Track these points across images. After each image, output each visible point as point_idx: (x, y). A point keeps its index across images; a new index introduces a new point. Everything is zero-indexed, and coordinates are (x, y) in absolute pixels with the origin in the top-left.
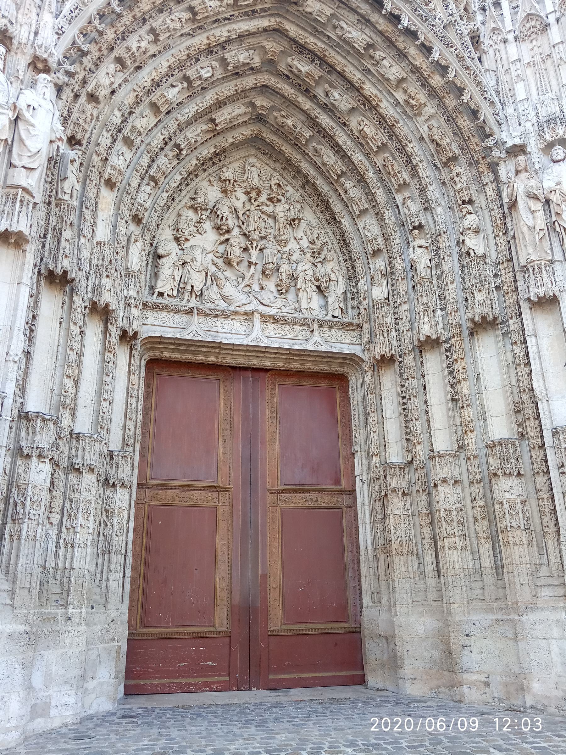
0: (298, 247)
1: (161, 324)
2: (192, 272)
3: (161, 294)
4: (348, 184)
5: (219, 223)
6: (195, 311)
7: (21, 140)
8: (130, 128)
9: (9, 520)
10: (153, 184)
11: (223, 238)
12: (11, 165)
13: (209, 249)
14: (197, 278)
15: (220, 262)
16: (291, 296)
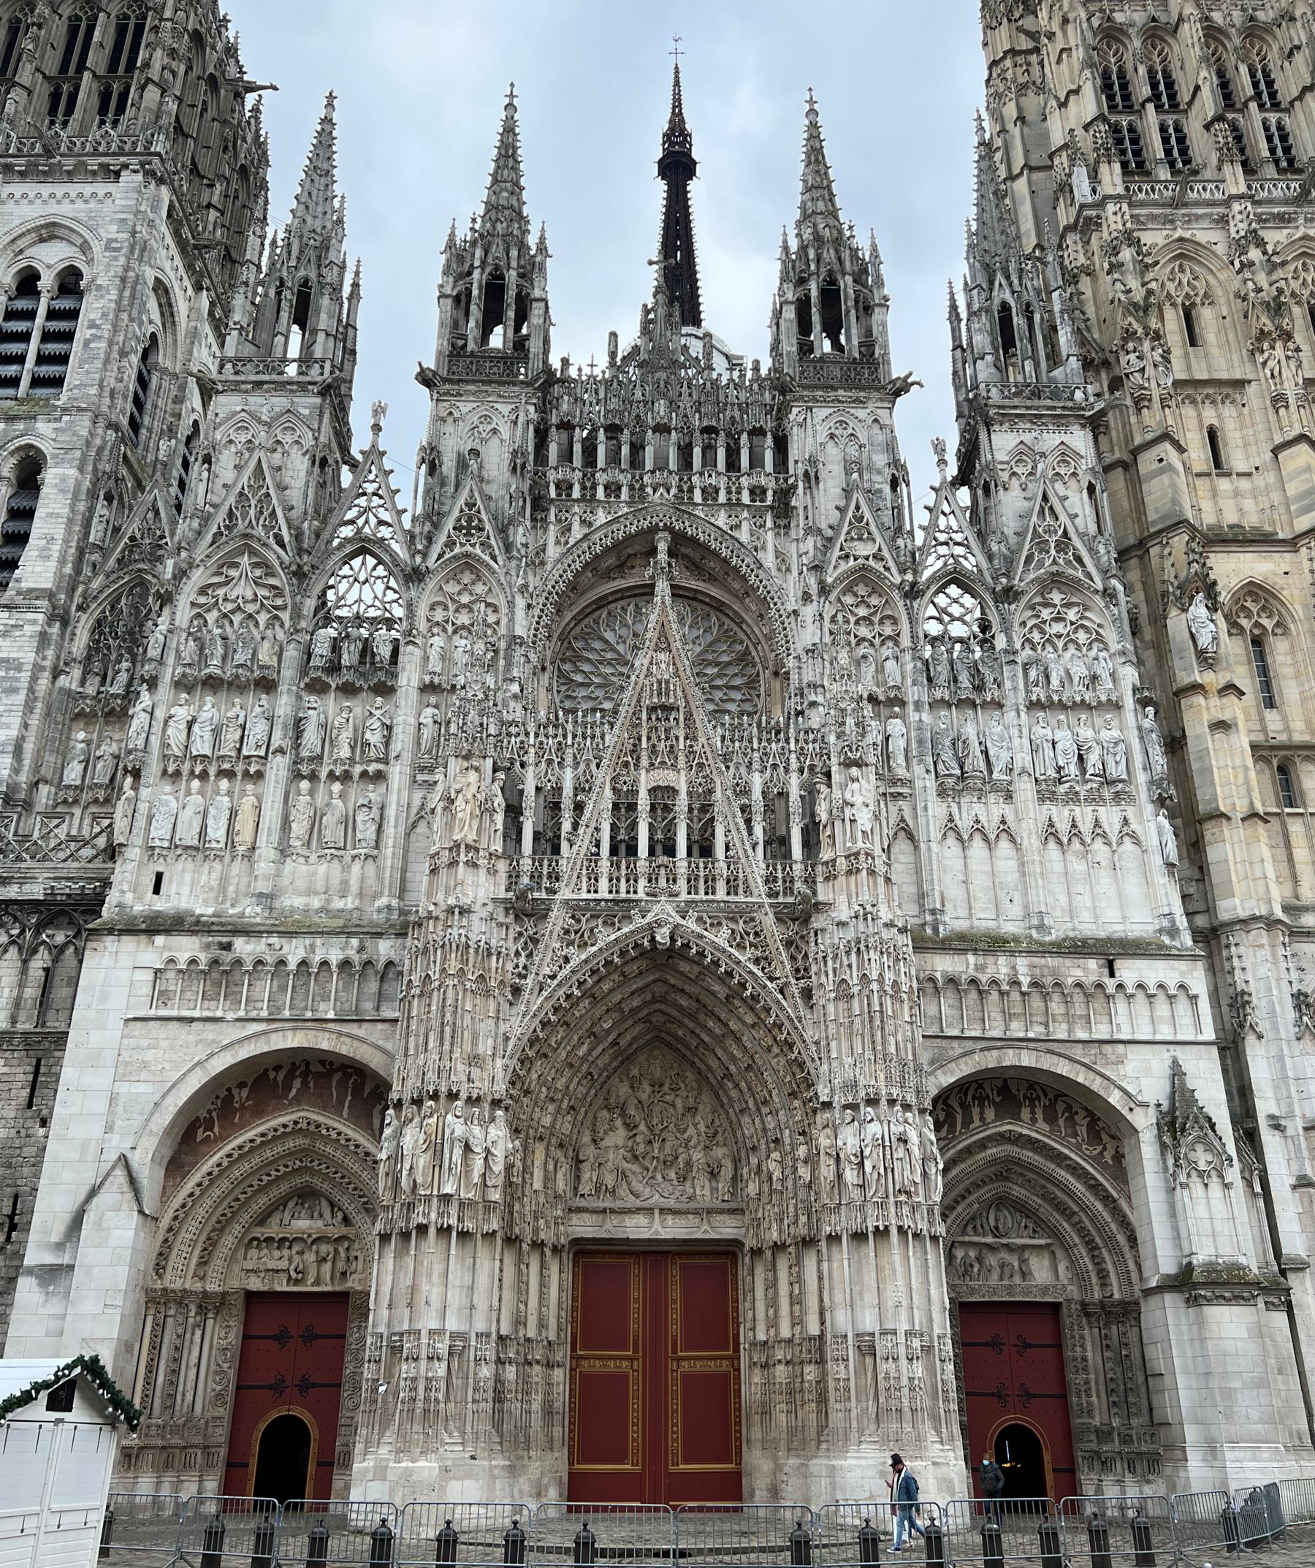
4: (730, 1085)
15: (628, 1155)
16: (688, 1184)
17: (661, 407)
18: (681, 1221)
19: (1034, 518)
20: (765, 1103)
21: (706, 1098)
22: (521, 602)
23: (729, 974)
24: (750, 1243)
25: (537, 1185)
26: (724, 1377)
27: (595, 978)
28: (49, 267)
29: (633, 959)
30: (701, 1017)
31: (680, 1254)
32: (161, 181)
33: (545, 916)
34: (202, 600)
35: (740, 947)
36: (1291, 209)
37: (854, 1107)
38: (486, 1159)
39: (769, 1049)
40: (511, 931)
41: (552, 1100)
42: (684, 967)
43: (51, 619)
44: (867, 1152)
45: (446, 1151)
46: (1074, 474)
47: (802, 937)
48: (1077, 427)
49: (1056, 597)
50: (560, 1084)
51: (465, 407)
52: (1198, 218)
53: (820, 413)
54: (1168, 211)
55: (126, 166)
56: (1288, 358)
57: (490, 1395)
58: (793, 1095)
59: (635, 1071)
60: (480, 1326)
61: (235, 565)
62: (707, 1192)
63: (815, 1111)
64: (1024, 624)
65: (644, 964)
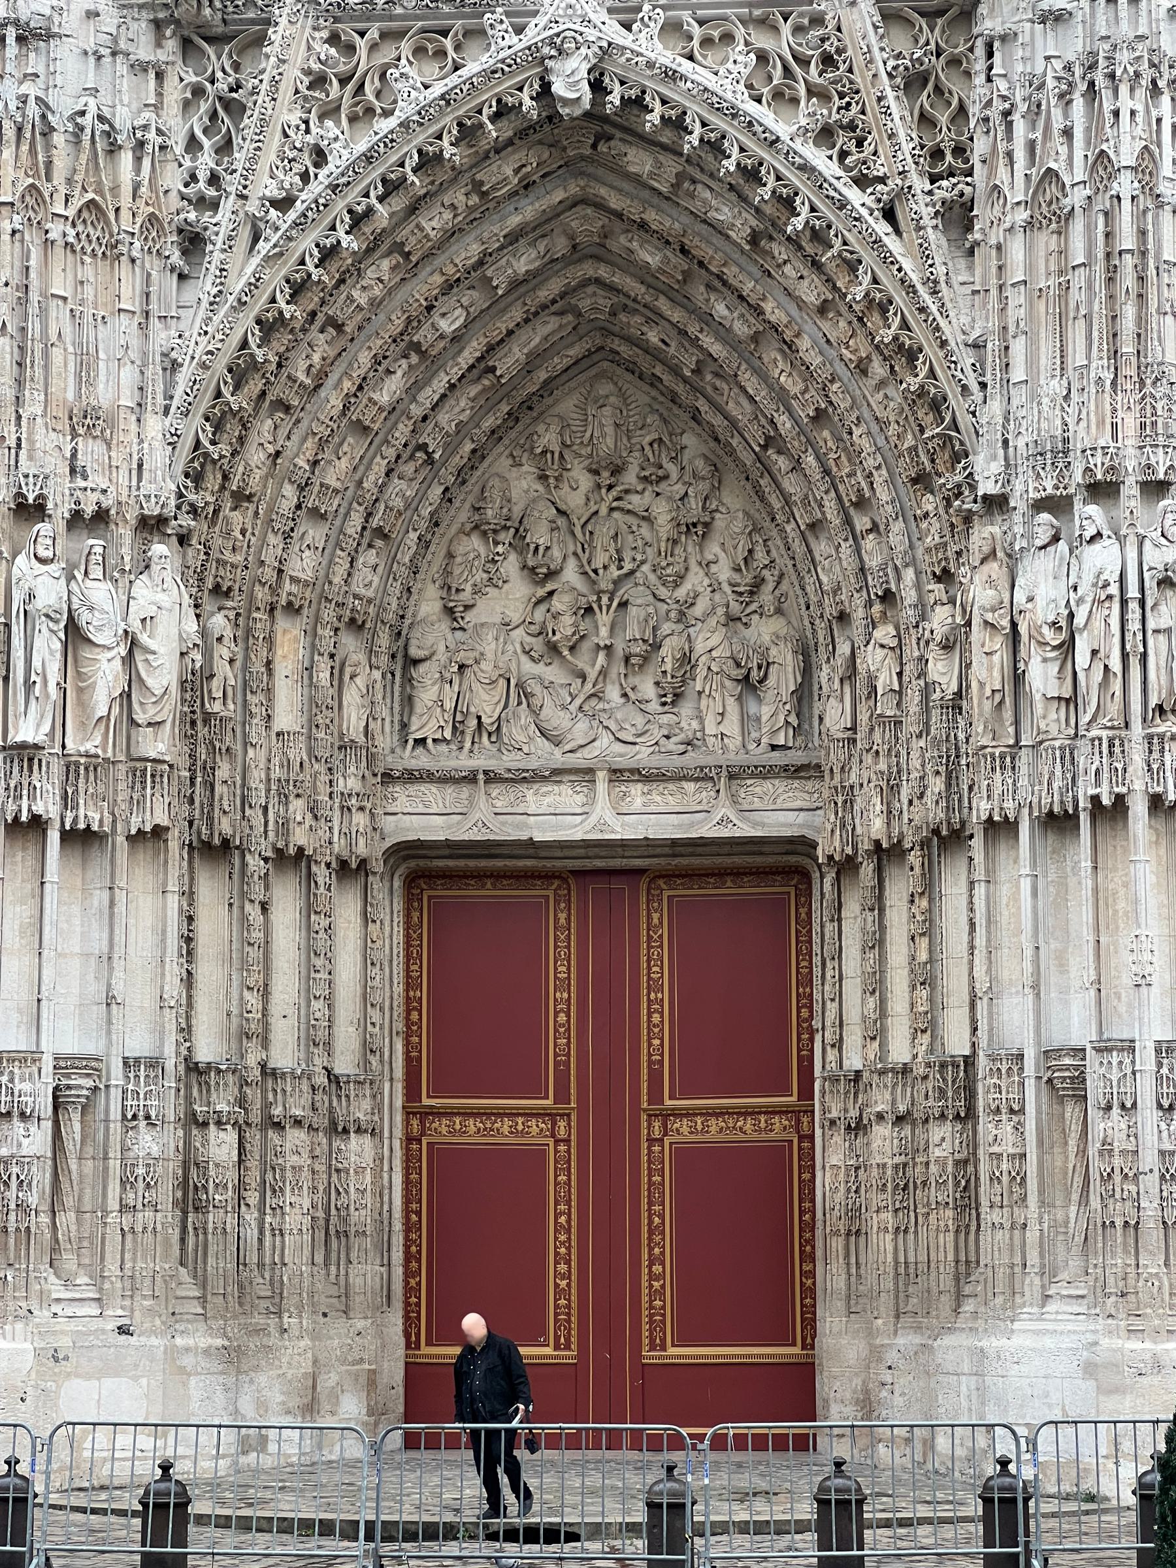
0: (706, 582)
1: (421, 809)
2: (476, 686)
3: (421, 742)
4: (783, 463)
5: (530, 563)
6: (481, 776)
7: (141, 681)
8: (316, 489)
9: (190, 1209)
10: (379, 543)
11: (541, 592)
12: (133, 722)
13: (516, 618)
14: (487, 698)
15: (537, 644)
16: (686, 709)
18: (664, 798)
20: (861, 503)
21: (733, 499)
23: (752, 174)
24: (828, 845)
25: (287, 716)
26: (776, 1155)
27: (399, 202)
29: (499, 149)
30: (698, 292)
31: (670, 876)
33: (260, 40)
35: (782, 98)
37: (1058, 505)
38: (129, 660)
39: (862, 368)
40: (171, 82)
41: (317, 515)
42: (639, 161)
44: (1079, 621)
45: (17, 642)
47: (954, 62)
50: (335, 474)
57: (166, 1194)
58: (922, 481)
59: (548, 438)
60: (138, 1044)
62: (732, 726)
63: (968, 518)
65: (530, 158)
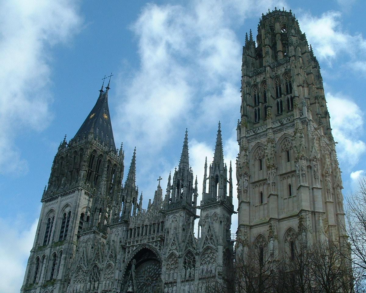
17: (147, 220)
19: (207, 233)
22: (117, 272)
28: (67, 212)
32: (82, 190)
34: (75, 279)
36: (282, 127)
43: (61, 284)
46: (217, 219)
48: (219, 207)
49: (209, 251)
51: (114, 230)
52: (262, 136)
53: (171, 216)
54: (255, 136)
55: (75, 190)
56: (272, 173)
61: (79, 272)
64: (202, 259)
